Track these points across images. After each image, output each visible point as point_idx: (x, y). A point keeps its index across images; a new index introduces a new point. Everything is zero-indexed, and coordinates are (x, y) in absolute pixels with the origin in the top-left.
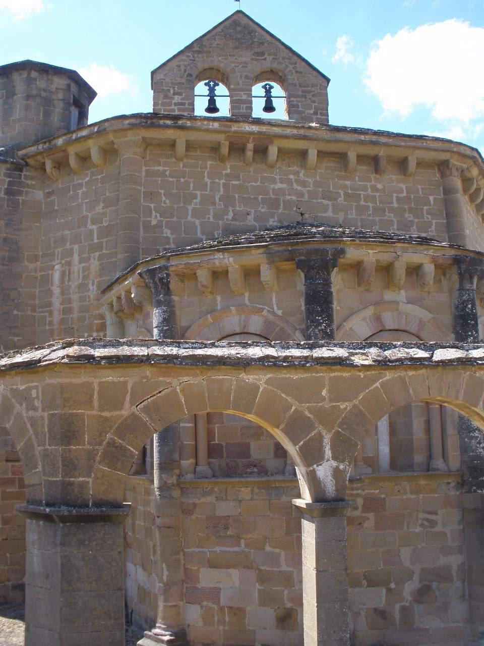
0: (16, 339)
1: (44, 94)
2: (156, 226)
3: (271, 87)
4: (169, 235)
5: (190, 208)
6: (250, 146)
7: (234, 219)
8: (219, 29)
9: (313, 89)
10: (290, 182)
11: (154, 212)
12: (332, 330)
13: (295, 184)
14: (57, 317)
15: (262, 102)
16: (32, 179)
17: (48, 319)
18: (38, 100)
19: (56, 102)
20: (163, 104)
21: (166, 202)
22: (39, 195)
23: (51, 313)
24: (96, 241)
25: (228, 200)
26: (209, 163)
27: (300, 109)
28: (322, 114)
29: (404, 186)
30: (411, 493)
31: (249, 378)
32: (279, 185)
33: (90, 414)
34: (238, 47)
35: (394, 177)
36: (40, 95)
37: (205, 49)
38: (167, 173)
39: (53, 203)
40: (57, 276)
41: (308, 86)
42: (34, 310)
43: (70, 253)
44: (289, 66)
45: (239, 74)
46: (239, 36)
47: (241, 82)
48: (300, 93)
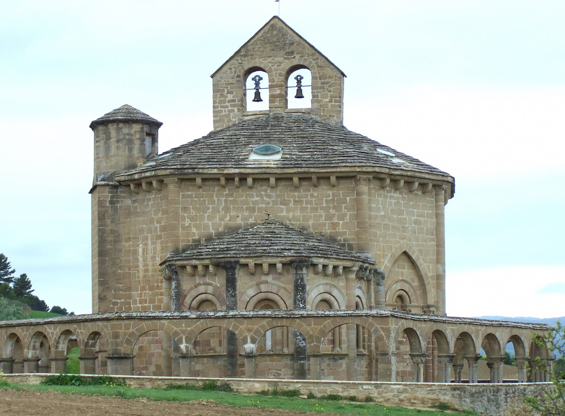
0: (120, 286)
1: (127, 137)
2: (188, 227)
3: (302, 78)
4: (195, 231)
5: (206, 215)
6: (237, 179)
7: (230, 220)
8: (260, 34)
9: (330, 80)
10: (262, 196)
11: (187, 219)
12: (235, 294)
13: (265, 198)
14: (141, 274)
15: (303, 82)
16: (124, 192)
17: (137, 275)
18: (124, 142)
19: (135, 141)
20: (220, 102)
21: (193, 212)
22: (128, 202)
23: (138, 271)
24: (159, 233)
25: (226, 209)
26: (216, 188)
27: (319, 98)
28: (336, 101)
29: (330, 193)
30: (270, 361)
31: (163, 321)
32: (256, 199)
33: (121, 331)
34: (276, 46)
35: (325, 187)
36: (125, 138)
37: (249, 53)
38: (194, 196)
39: (136, 208)
40: (140, 250)
41: (326, 78)
42: (129, 269)
43: (146, 238)
44: (313, 61)
45: (274, 72)
46: (275, 39)
47: (276, 80)
48: (320, 85)
